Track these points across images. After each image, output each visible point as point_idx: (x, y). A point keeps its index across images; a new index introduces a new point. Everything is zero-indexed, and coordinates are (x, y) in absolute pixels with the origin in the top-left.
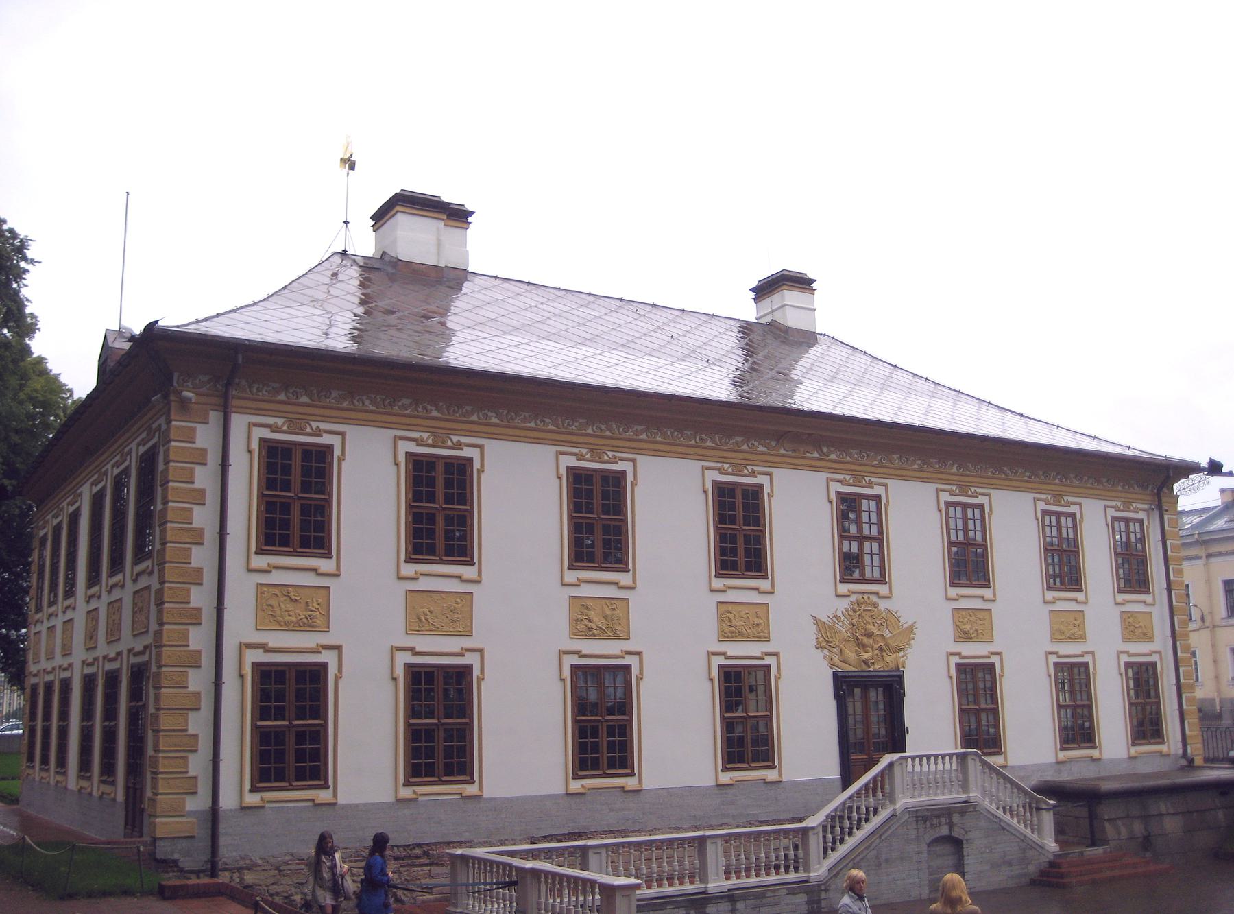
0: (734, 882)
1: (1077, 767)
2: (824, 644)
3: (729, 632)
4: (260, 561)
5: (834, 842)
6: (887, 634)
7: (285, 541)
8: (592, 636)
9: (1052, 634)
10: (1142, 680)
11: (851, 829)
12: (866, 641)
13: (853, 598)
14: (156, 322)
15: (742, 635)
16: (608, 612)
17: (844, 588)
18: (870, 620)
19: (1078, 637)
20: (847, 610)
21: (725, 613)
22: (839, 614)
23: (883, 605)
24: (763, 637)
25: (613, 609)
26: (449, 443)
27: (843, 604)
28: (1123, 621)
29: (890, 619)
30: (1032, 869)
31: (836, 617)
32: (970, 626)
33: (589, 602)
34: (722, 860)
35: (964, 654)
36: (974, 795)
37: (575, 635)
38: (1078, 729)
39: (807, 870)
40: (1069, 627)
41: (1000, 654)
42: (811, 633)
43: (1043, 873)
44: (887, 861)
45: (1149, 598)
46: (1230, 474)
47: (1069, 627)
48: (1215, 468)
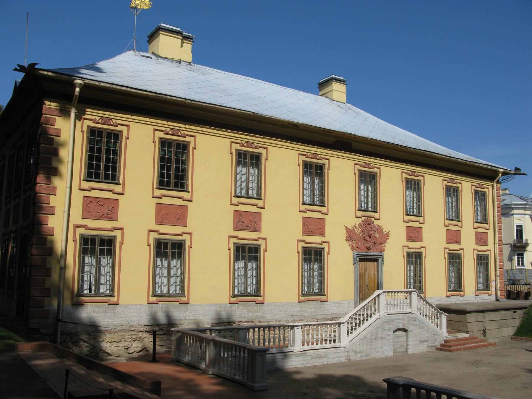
0: (306, 347)
1: (454, 301)
2: (349, 239)
3: (307, 231)
4: (86, 185)
5: (352, 330)
6: (377, 236)
7: (97, 176)
8: (244, 230)
9: (447, 240)
10: (482, 261)
11: (360, 324)
12: (368, 238)
13: (363, 218)
14: (36, 64)
15: (313, 233)
16: (251, 218)
17: (360, 214)
18: (370, 229)
19: (458, 242)
20: (360, 224)
21: (306, 221)
22: (357, 226)
23: (376, 223)
24: (323, 234)
25: (254, 218)
26: (180, 134)
27: (359, 221)
28: (476, 236)
29: (379, 229)
30: (437, 344)
31: (355, 226)
32: (414, 234)
33: (243, 214)
34: (301, 337)
35: (410, 247)
36: (414, 309)
37: (236, 229)
38: (456, 283)
39: (340, 342)
40: (454, 237)
41: (424, 247)
42: (343, 234)
43: (441, 345)
44: (375, 339)
45: (487, 226)
46: (524, 174)
47: (454, 237)
48: (517, 171)
